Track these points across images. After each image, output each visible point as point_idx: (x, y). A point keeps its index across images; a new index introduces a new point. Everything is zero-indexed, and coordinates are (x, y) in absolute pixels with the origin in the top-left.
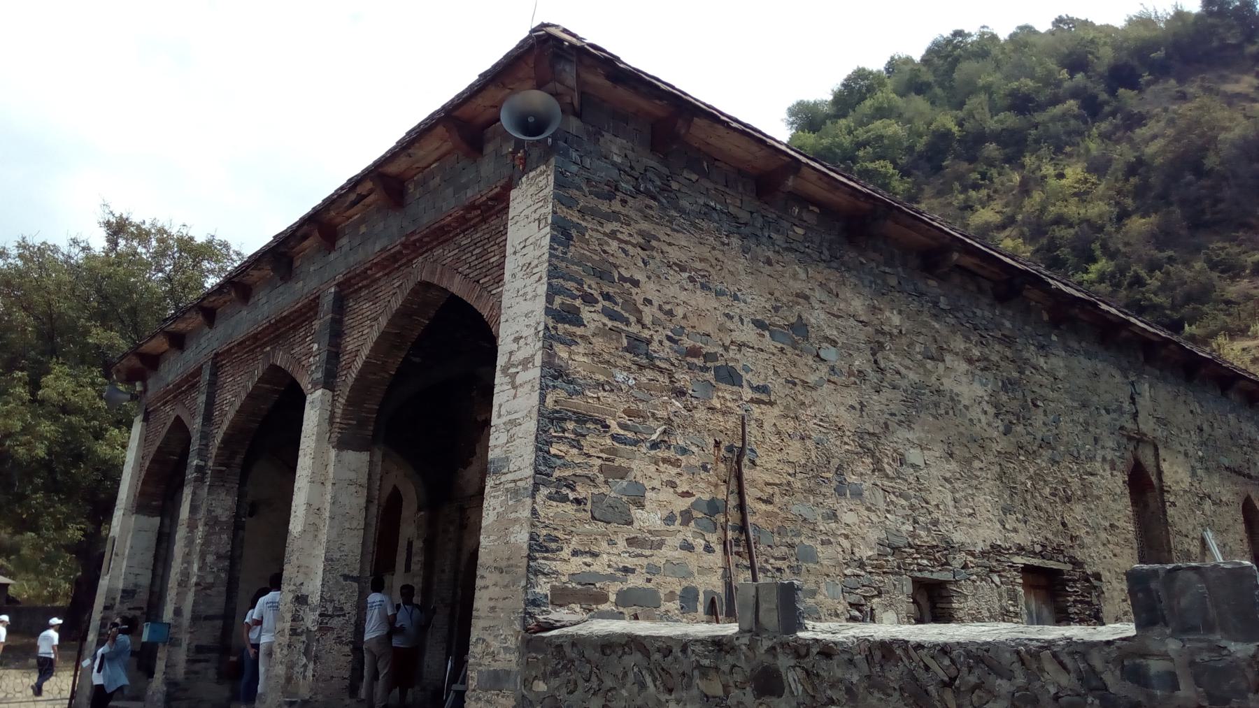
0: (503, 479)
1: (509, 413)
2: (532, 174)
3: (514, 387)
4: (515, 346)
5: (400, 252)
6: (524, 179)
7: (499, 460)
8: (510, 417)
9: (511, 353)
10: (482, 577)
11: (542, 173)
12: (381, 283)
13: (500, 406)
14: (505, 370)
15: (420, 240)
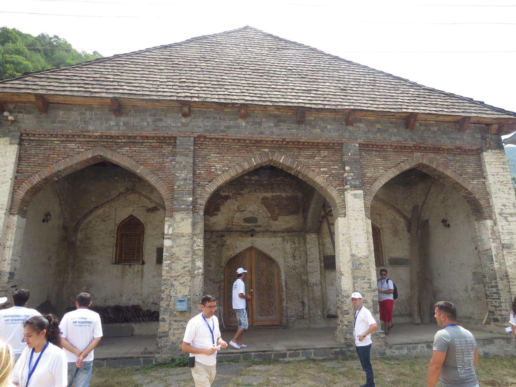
0: (512, 251)
1: (508, 229)
2: (493, 151)
3: (507, 221)
4: (503, 208)
5: (410, 147)
6: (490, 151)
7: (508, 244)
8: (508, 231)
9: (502, 209)
10: (512, 282)
11: (498, 153)
12: (389, 153)
13: (502, 226)
14: (501, 214)
15: (425, 148)
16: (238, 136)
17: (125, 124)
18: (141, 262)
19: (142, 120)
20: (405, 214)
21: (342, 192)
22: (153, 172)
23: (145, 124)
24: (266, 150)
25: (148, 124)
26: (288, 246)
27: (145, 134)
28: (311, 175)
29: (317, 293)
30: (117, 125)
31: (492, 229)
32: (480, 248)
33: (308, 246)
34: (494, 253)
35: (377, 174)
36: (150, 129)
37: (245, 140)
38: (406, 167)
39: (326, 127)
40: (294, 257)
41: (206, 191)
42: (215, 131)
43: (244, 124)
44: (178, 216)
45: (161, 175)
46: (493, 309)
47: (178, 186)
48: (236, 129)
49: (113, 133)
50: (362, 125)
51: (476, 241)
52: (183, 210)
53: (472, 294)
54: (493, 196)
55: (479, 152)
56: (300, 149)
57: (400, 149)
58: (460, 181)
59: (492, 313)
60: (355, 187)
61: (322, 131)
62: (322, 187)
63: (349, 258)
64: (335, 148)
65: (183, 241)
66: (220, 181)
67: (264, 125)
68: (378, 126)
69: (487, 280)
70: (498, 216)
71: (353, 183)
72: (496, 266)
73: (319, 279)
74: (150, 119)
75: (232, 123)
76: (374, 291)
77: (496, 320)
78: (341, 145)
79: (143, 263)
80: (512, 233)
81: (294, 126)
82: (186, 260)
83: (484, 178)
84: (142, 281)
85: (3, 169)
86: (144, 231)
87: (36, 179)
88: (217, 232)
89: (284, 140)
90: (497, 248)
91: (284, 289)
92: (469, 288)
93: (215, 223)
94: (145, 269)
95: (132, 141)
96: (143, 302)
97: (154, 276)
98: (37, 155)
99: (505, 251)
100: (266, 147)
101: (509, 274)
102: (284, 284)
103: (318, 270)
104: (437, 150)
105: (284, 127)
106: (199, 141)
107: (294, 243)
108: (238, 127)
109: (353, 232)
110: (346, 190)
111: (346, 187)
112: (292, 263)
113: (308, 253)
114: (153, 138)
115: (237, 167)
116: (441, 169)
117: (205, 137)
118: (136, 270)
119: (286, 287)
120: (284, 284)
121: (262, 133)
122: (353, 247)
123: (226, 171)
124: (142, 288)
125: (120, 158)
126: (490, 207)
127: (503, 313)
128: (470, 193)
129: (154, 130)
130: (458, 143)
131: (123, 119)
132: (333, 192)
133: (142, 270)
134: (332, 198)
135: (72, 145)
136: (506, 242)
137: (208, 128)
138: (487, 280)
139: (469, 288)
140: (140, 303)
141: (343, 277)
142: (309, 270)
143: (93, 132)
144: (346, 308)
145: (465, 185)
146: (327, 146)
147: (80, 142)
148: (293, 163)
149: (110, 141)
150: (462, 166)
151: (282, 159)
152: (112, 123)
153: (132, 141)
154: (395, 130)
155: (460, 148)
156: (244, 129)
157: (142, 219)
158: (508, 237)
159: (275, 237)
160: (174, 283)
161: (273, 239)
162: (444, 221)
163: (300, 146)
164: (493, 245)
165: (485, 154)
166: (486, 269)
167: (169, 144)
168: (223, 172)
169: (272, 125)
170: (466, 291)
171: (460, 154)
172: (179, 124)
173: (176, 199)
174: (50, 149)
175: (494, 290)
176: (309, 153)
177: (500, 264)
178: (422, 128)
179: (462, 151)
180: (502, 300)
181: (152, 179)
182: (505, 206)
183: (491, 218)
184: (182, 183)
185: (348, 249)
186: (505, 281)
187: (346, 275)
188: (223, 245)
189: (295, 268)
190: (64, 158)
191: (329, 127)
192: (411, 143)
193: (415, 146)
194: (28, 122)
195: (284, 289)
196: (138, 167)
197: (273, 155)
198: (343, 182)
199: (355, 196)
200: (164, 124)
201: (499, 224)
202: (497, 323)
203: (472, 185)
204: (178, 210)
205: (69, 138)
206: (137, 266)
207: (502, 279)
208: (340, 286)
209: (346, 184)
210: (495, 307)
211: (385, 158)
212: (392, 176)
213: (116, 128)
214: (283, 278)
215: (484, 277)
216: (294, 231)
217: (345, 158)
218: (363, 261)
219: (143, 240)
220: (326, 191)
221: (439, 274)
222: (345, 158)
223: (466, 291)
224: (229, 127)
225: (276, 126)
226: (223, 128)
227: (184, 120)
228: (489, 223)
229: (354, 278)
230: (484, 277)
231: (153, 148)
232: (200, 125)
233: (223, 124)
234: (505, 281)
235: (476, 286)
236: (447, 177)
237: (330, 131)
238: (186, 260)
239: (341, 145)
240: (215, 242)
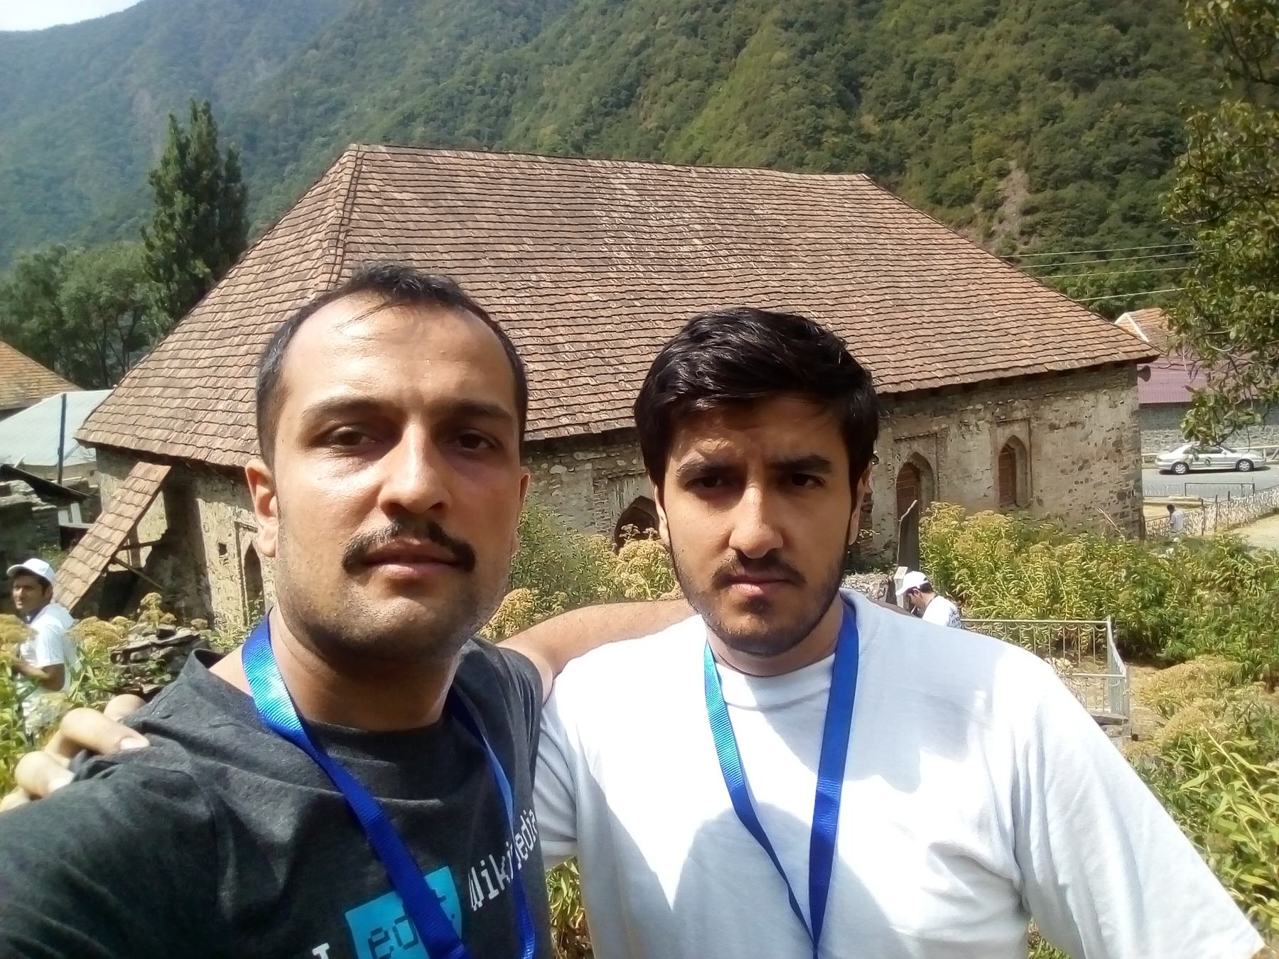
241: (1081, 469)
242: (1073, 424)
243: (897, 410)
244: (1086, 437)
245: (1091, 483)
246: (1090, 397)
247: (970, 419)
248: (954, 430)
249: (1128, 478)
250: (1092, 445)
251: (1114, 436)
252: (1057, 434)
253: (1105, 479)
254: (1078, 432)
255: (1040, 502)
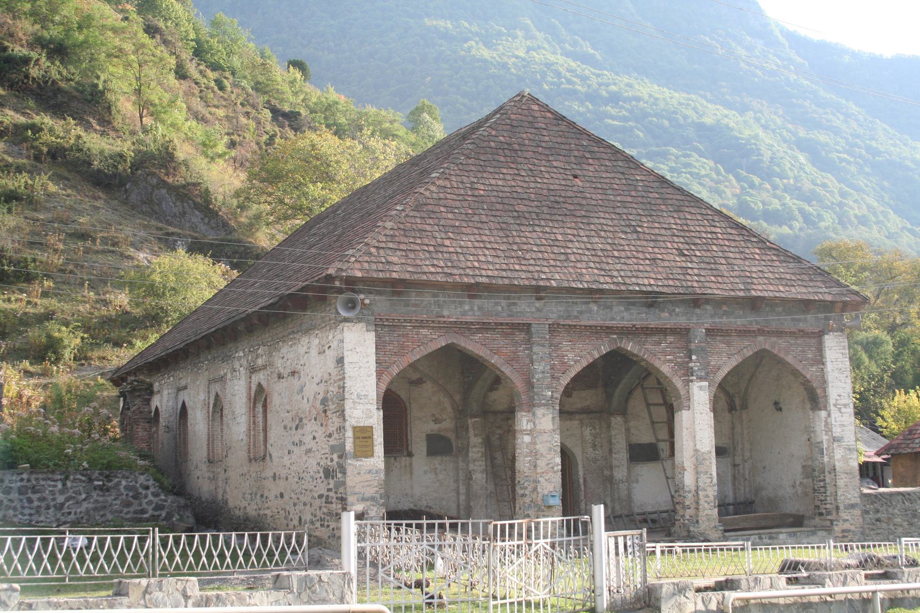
14: (835, 405)
16: (591, 323)
17: (480, 308)
18: (405, 453)
19: (497, 304)
20: (727, 388)
21: (687, 383)
22: (507, 362)
23: (500, 308)
24: (615, 336)
25: (503, 308)
26: (587, 432)
27: (500, 320)
28: (657, 364)
29: (624, 493)
30: (472, 309)
31: (826, 421)
32: (812, 440)
33: (613, 433)
34: (825, 446)
35: (721, 362)
36: (504, 314)
37: (596, 327)
38: (748, 353)
39: (674, 310)
40: (594, 446)
41: (560, 384)
42: (568, 317)
43: (595, 308)
44: (539, 412)
45: (516, 366)
46: (818, 503)
47: (538, 380)
48: (588, 315)
49: (469, 319)
50: (709, 307)
51: (809, 430)
52: (544, 405)
53: (800, 490)
54: (830, 385)
55: (820, 335)
56: (647, 334)
57: (743, 333)
58: (800, 368)
59: (818, 507)
60: (701, 379)
61: (671, 315)
62: (666, 377)
63: (692, 453)
64: (683, 333)
65: (546, 437)
66: (573, 373)
67: (615, 309)
68: (725, 308)
69: (816, 474)
70: (832, 407)
71: (699, 374)
72: (826, 459)
73: (626, 474)
74: (504, 303)
75: (584, 307)
76: (714, 485)
77: (821, 514)
78: (688, 330)
79: (410, 455)
80: (843, 425)
81: (644, 309)
82: (549, 457)
83: (823, 364)
84: (411, 478)
85: (365, 360)
86: (406, 409)
87: (395, 370)
88: (502, 412)
89: (634, 326)
90: (828, 440)
91: (582, 488)
92: (798, 483)
93: (495, 400)
94: (414, 463)
95: (485, 327)
96: (415, 506)
97: (425, 472)
98: (391, 342)
99: (836, 444)
100: (615, 334)
101: (837, 467)
102: (581, 481)
103: (625, 462)
104: (779, 333)
105: (634, 310)
106: (554, 329)
107: (594, 428)
108: (590, 311)
109: (697, 427)
110: (692, 381)
111: (691, 378)
112: (593, 455)
113: (614, 441)
114: (507, 324)
115: (588, 356)
116: (782, 355)
117: (558, 324)
118: (403, 464)
119: (585, 485)
120: (581, 481)
121: (613, 319)
122: (698, 443)
123: (578, 361)
124: (412, 487)
125: (473, 345)
126: (826, 397)
127: (828, 506)
128: (808, 381)
129: (509, 316)
130: (801, 326)
131: (477, 302)
132: (678, 383)
133: (411, 465)
134: (676, 389)
135: (424, 331)
136: (837, 435)
137: (562, 313)
138: (816, 474)
139: (798, 483)
140: (412, 506)
141: (686, 473)
142: (615, 463)
143: (449, 317)
144: (687, 503)
145: (804, 373)
146: (674, 331)
147: (433, 328)
148: (640, 350)
149: (464, 327)
150: (803, 351)
151: (630, 346)
152: (467, 307)
153: (485, 327)
154: (741, 312)
155: (802, 331)
156: (595, 315)
157: (403, 395)
158: (839, 430)
159: (571, 420)
160: (540, 479)
161: (568, 422)
162: (776, 403)
163: (648, 331)
164: (825, 438)
165: (826, 337)
166: (817, 463)
167: (521, 331)
168: (576, 362)
169: (623, 309)
170: (794, 486)
171: (802, 337)
172: (534, 310)
173: (537, 394)
174: (403, 336)
175: (822, 484)
176: (656, 338)
177: (830, 458)
178: (768, 309)
179: (803, 334)
180: (828, 493)
181: (507, 370)
182: (839, 396)
183: (825, 408)
184: (540, 376)
185: (691, 444)
186: (833, 474)
187: (689, 470)
188: (509, 431)
189: (595, 460)
190: (419, 346)
191: (677, 310)
192: (755, 327)
193: (759, 330)
194: (381, 304)
195: (582, 488)
196: (492, 357)
197: (621, 342)
198: (689, 372)
199: (701, 388)
200: (518, 310)
201: (833, 415)
202: (822, 517)
203: (810, 372)
204: (540, 405)
205: (422, 324)
206: (404, 459)
207: (830, 473)
208: (682, 482)
209: (692, 375)
210: (821, 501)
211: (729, 344)
212: (735, 364)
213: (470, 313)
214: (581, 473)
215: (814, 470)
216: (591, 412)
217: (693, 346)
218: (706, 456)
219: (406, 425)
220: (671, 381)
221: (764, 468)
222: (693, 346)
223: (794, 486)
224: (581, 312)
225: (627, 310)
226: (575, 313)
227: (538, 304)
228: (823, 414)
229: (697, 473)
230: (814, 470)
231: (505, 335)
232: (554, 311)
233: (575, 310)
234: (833, 474)
235: (805, 481)
236: (788, 363)
237: (677, 315)
238: (549, 457)
239: (688, 330)
240: (500, 427)
241: (297, 429)
242: (293, 373)
243: (209, 357)
244: (301, 390)
245: (304, 448)
246: (305, 340)
247: (237, 365)
248: (229, 376)
249: (333, 449)
250: (305, 400)
251: (321, 389)
252: (283, 384)
253: (312, 445)
254: (295, 382)
255: (270, 455)
